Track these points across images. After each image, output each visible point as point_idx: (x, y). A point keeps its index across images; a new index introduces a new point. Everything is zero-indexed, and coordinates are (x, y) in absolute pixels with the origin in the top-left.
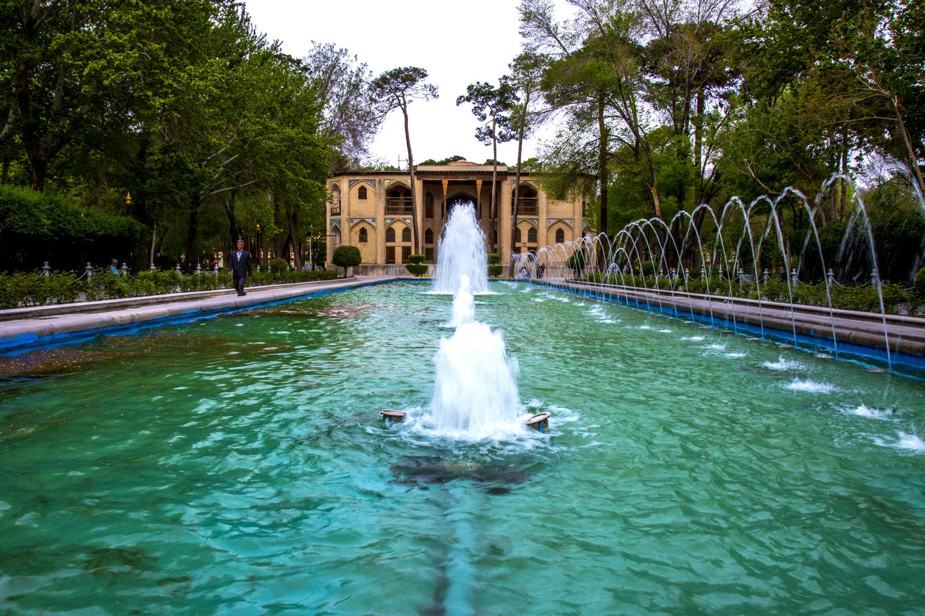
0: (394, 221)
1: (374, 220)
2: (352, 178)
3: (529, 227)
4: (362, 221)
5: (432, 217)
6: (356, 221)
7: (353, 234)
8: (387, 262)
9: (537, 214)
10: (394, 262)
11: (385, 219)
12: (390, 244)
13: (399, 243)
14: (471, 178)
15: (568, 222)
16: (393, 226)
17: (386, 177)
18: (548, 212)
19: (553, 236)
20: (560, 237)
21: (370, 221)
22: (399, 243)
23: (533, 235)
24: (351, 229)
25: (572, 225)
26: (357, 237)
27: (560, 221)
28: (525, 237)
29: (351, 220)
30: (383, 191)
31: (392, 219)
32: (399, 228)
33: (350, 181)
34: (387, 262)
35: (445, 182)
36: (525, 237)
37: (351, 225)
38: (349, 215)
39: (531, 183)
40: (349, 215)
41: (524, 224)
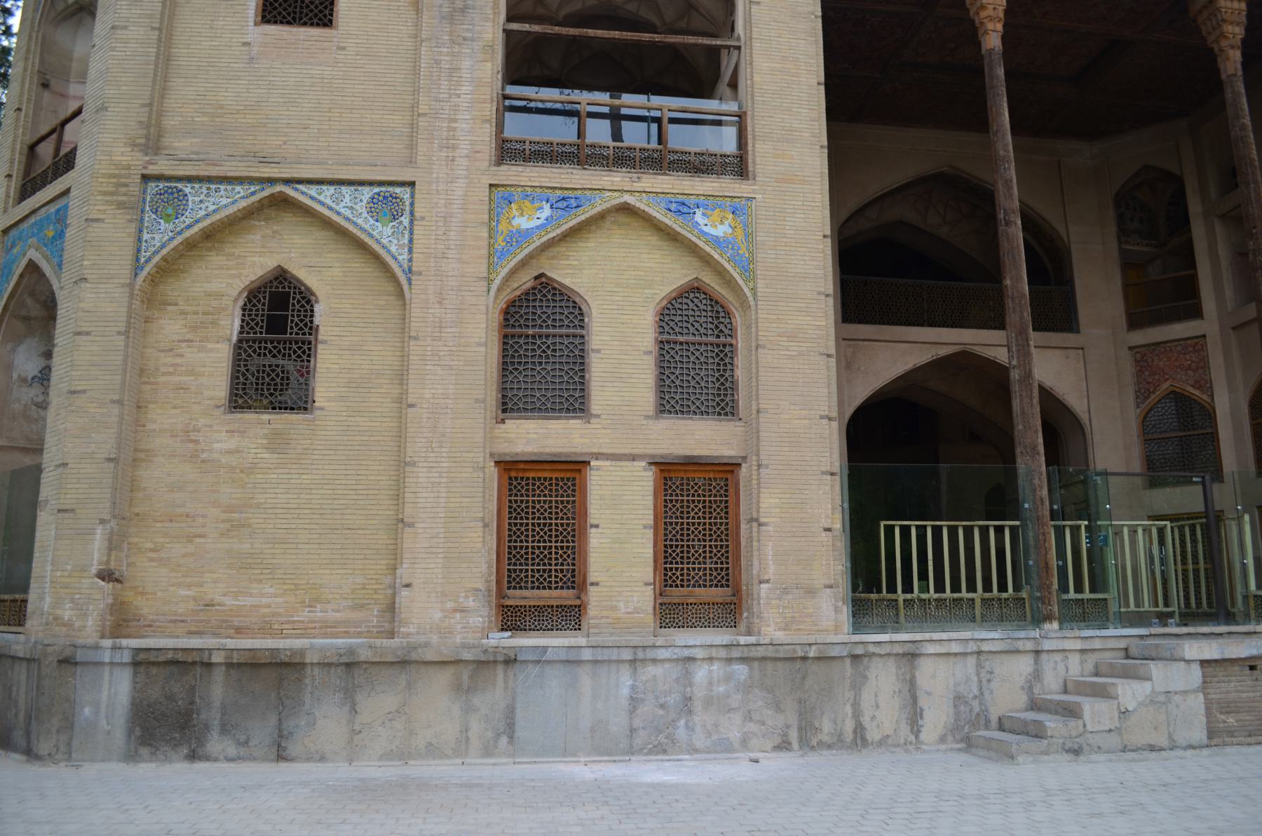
1: (391, 196)
4: (279, 206)
6: (207, 205)
7: (170, 327)
8: (512, 618)
10: (571, 616)
12: (536, 436)
13: (621, 431)
16: (577, 271)
21: (351, 207)
22: (621, 431)
26: (213, 363)
29: (166, 189)
31: (564, 201)
32: (623, 299)
34: (512, 618)
37: (162, 236)
38: (152, 143)
40: (152, 143)
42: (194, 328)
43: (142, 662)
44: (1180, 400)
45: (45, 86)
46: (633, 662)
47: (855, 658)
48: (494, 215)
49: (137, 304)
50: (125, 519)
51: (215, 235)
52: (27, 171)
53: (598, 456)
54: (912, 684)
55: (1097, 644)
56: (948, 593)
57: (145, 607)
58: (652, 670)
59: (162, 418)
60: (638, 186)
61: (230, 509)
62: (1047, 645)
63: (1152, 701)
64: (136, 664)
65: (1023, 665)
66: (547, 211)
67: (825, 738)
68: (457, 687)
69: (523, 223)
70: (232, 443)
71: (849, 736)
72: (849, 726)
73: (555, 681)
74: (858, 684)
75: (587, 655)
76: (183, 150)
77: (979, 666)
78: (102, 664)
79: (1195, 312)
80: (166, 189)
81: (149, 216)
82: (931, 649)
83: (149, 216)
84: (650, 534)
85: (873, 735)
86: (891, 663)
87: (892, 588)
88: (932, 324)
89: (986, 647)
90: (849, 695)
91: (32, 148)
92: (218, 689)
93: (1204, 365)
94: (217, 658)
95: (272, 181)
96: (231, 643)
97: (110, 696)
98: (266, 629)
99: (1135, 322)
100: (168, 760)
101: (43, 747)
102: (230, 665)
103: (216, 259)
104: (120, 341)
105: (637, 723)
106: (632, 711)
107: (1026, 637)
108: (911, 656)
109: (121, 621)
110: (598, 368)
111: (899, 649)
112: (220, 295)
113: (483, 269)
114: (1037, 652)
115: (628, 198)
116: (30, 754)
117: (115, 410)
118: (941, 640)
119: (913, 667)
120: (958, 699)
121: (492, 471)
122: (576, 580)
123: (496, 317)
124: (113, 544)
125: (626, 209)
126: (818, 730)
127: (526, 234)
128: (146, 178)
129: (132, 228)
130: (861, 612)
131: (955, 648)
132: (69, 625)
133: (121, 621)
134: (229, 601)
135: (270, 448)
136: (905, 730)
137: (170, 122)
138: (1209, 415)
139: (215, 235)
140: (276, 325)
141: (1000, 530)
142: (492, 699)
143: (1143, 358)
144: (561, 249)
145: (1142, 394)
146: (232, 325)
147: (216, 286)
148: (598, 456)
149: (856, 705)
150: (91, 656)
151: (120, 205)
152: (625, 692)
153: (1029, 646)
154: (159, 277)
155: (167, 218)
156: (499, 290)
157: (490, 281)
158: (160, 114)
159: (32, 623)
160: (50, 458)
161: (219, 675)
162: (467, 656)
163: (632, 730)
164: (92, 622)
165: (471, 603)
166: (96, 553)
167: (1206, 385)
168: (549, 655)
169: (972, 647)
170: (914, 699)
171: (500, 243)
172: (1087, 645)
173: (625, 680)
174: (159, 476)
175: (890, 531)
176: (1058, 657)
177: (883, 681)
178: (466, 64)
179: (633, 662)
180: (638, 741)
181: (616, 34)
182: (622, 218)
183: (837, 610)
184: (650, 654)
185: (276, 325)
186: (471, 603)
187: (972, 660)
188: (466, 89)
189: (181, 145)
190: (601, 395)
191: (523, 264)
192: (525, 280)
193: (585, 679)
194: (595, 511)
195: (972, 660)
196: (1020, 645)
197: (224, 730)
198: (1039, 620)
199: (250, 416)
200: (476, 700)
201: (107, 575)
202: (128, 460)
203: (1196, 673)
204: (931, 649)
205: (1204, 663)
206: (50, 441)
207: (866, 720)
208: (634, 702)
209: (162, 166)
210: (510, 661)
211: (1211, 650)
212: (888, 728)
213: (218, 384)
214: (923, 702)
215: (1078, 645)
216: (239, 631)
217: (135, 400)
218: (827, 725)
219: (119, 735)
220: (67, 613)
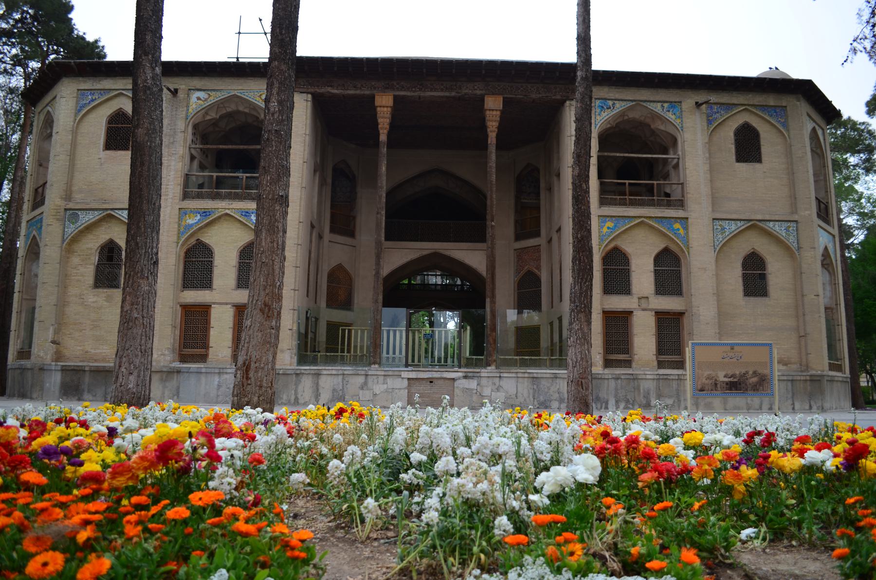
0: (211, 221)
2: (87, 84)
3: (659, 245)
5: (351, 234)
6: (86, 218)
7: (75, 260)
8: (183, 359)
9: (681, 204)
10: (203, 358)
11: (183, 213)
12: (194, 296)
14: (470, 89)
15: (778, 229)
16: (211, 238)
17: (196, 82)
18: (715, 201)
19: (734, 276)
20: (755, 278)
23: (670, 271)
24: (71, 244)
25: (792, 241)
26: (88, 272)
27: (754, 226)
28: (643, 276)
29: (72, 214)
30: (181, 125)
31: (205, 213)
33: (81, 92)
35: (384, 102)
36: (643, 276)
37: (71, 229)
38: (68, 197)
39: (657, 108)
40: (68, 197)
41: (640, 234)
42: (83, 260)
43: (64, 370)
44: (530, 273)
45: (41, 165)
46: (219, 373)
47: (297, 374)
48: (180, 219)
49: (64, 253)
50: (60, 324)
51: (90, 228)
52: (35, 199)
53: (214, 303)
54: (317, 384)
55: (390, 373)
56: (345, 354)
57: (66, 353)
58: (226, 376)
59: (73, 291)
60: (231, 207)
61: (93, 321)
62: (370, 373)
63: (386, 391)
64: (62, 370)
65: (361, 380)
66: (199, 217)
67: (284, 401)
68: (163, 381)
69: (190, 221)
70: (94, 299)
71: (293, 401)
72: (293, 398)
73: (193, 379)
74: (297, 385)
75: (203, 370)
76: (79, 199)
77: (343, 379)
78: (51, 370)
79: (537, 234)
80: (72, 214)
81: (67, 223)
82: (325, 372)
83: (67, 223)
84: (231, 330)
85: (301, 401)
86: (310, 376)
87: (343, 351)
88: (421, 241)
89: (346, 372)
90: (294, 387)
91: (36, 190)
92: (87, 379)
93: (538, 259)
94: (87, 369)
95: (107, 209)
96: (91, 364)
97: (55, 380)
98: (104, 360)
99: (518, 237)
100: (71, 400)
101: (34, 396)
102: (91, 371)
103: (90, 236)
104: (58, 266)
105: (220, 393)
106: (218, 389)
107: (362, 370)
108: (318, 375)
109: (58, 356)
110: (216, 272)
111: (313, 372)
112: (91, 249)
113: (175, 239)
114: (367, 375)
115: (228, 211)
116: (31, 398)
117: (56, 289)
118: (327, 370)
119: (318, 378)
120: (334, 390)
121: (179, 308)
122: (206, 346)
123: (182, 254)
124: (57, 332)
125: (227, 214)
126: (282, 398)
127: (192, 225)
128: (66, 210)
129: (62, 227)
130: (302, 359)
131: (334, 372)
132: (42, 358)
133: (58, 356)
134: (93, 351)
135: (107, 301)
136: (313, 399)
137: (75, 188)
138: (537, 281)
139: (90, 228)
140: (110, 259)
141: (395, 332)
142: (173, 383)
143: (520, 254)
144: (205, 230)
145: (517, 271)
146: (95, 259)
147: (90, 245)
148: (214, 303)
149: (296, 391)
150: (49, 368)
151: (58, 219)
152: (216, 383)
153: (363, 372)
154: (71, 244)
155: (73, 223)
156: (182, 245)
157: (178, 243)
158: (71, 186)
159: (32, 357)
160: (38, 304)
161: (87, 374)
162: (165, 369)
163: (218, 396)
164: (49, 357)
165: (166, 352)
166: (50, 335)
167: (539, 268)
168: (191, 370)
169: (341, 372)
170: (318, 390)
171: (182, 229)
172: (386, 373)
173: (216, 379)
174: (73, 310)
175: (343, 331)
176: (375, 377)
177: (307, 383)
178: (173, 163)
179: (219, 373)
180: (220, 399)
181: (230, 147)
182: (227, 218)
183: (291, 358)
184: (225, 371)
185: (110, 259)
186: (166, 352)
187: (340, 377)
188: (172, 173)
189: (77, 196)
190: (217, 282)
191: (192, 235)
192: (193, 241)
193: (203, 378)
194: (213, 322)
195: (340, 377)
196: (359, 372)
197: (89, 392)
198: (370, 364)
199: (100, 290)
200: (167, 384)
201: (53, 342)
202: (61, 305)
203: (406, 382)
204: (325, 372)
205: (409, 379)
206: (38, 298)
207: (299, 396)
208: (219, 386)
209: (71, 205)
210: (179, 372)
211: (413, 375)
212: (307, 399)
213: (90, 279)
214: (321, 391)
215: (383, 373)
216: (96, 361)
217: (63, 284)
218: (285, 397)
219: (57, 392)
220: (42, 355)
